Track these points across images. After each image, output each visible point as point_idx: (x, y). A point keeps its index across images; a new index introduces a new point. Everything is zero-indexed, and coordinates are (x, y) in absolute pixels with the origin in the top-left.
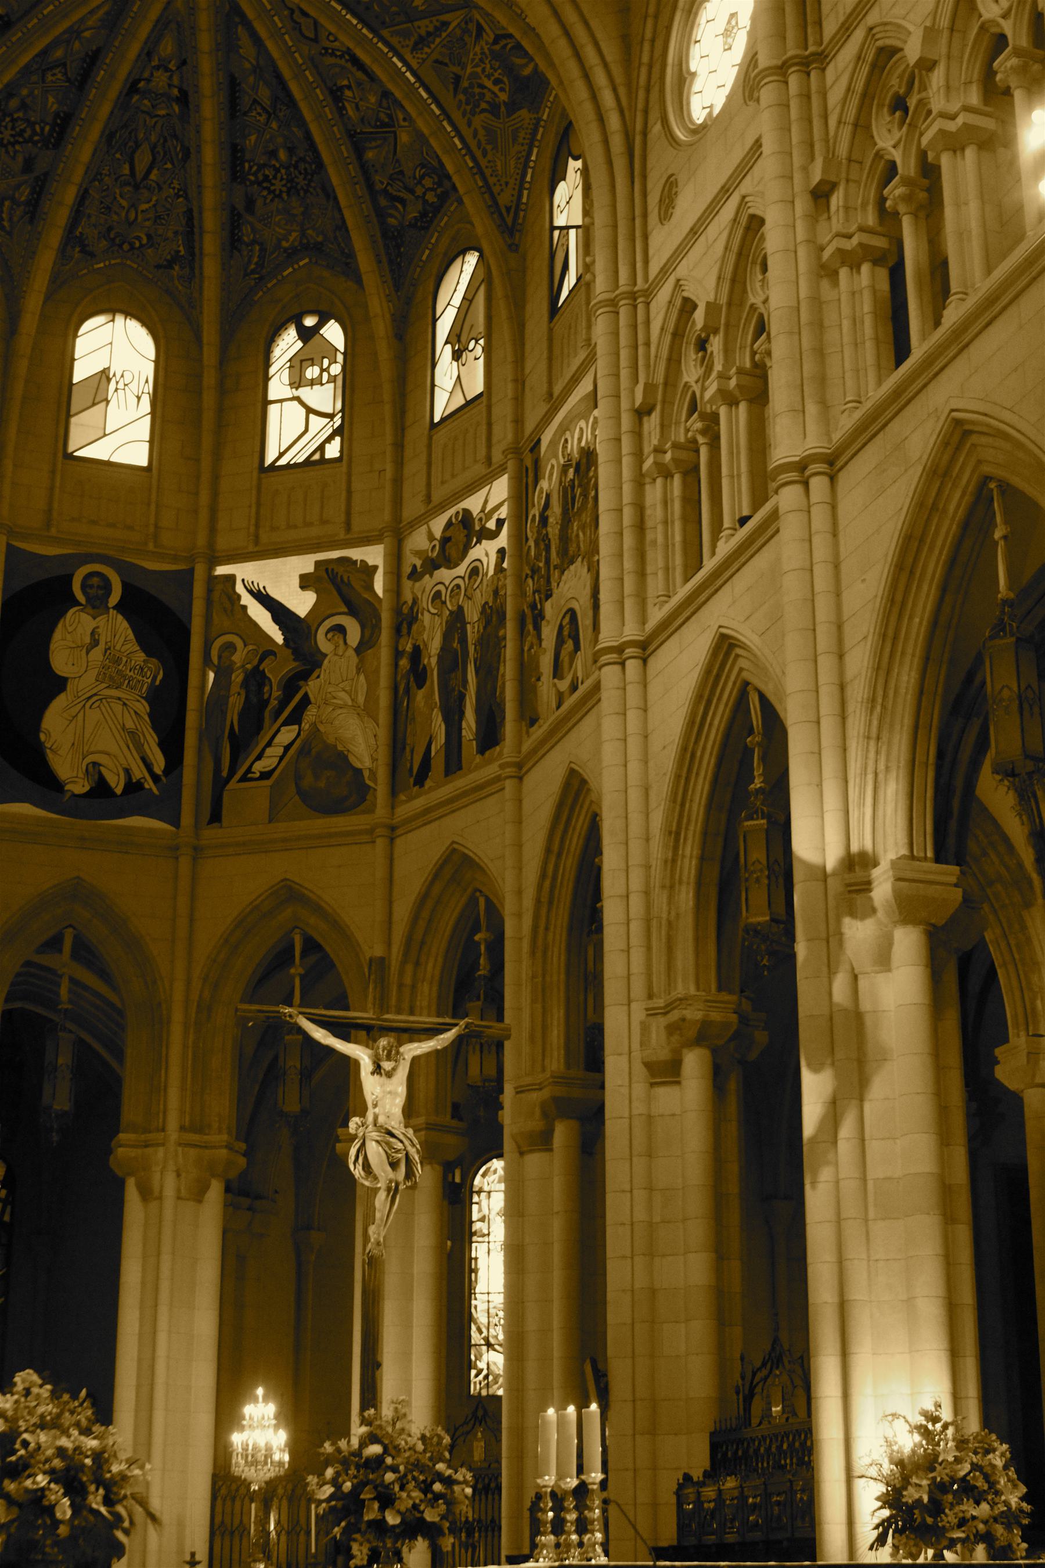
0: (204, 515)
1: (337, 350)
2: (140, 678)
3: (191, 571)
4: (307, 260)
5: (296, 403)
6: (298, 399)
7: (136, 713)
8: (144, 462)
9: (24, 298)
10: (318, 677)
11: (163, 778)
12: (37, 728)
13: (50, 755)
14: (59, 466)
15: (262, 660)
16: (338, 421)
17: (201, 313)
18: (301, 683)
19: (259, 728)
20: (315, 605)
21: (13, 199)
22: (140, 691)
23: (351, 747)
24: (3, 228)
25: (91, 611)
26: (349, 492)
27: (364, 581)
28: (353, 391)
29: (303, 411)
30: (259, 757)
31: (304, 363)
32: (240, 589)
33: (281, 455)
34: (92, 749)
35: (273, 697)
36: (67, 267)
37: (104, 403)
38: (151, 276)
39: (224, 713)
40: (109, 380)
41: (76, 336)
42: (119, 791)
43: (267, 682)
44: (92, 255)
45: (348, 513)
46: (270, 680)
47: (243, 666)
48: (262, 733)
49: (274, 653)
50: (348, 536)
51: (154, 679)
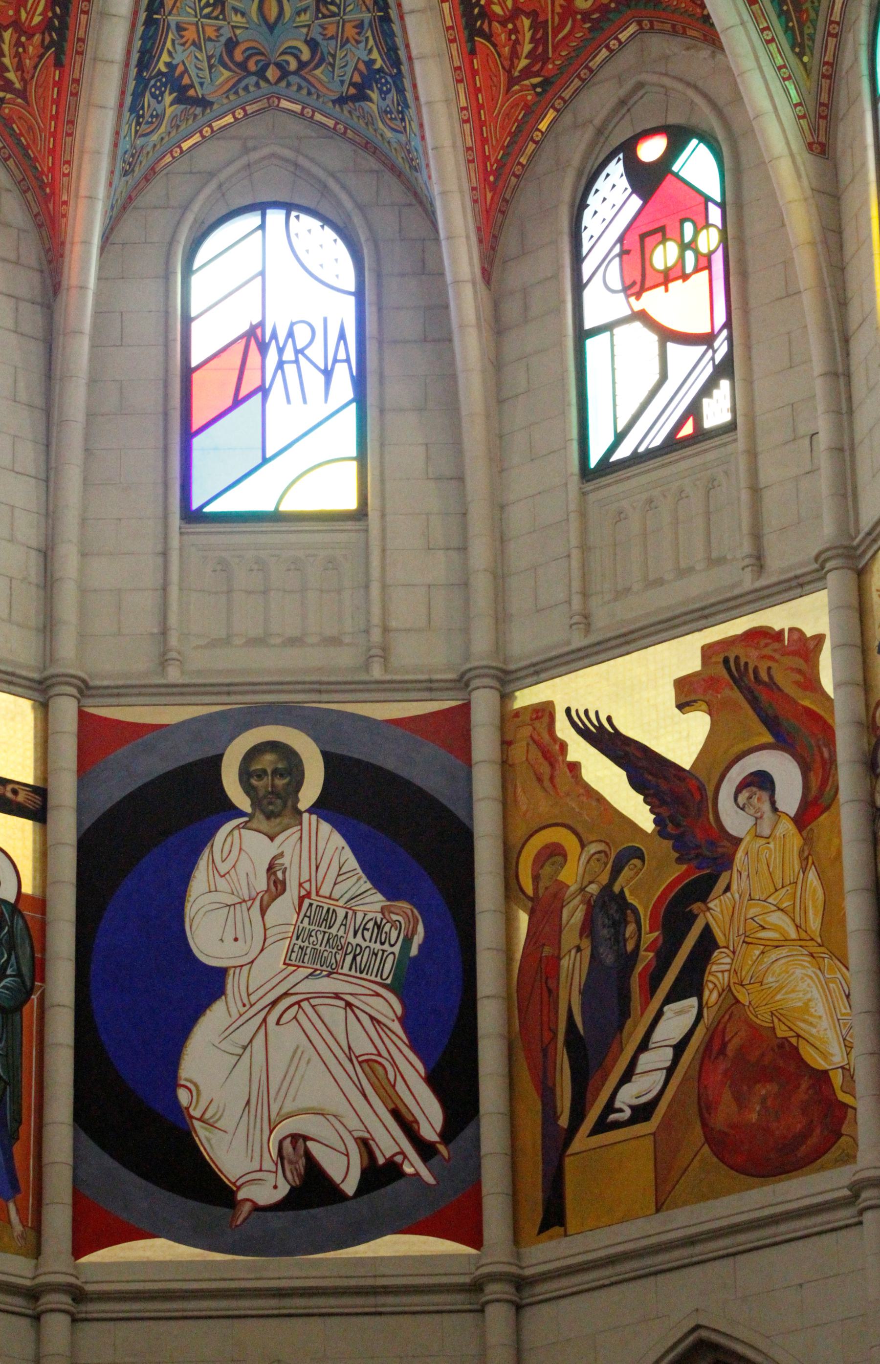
0: (482, 585)
1: (707, 199)
2: (378, 946)
3: (465, 709)
4: (632, 28)
5: (637, 325)
6: (642, 316)
7: (372, 1018)
8: (351, 504)
9: (64, 216)
10: (728, 889)
11: (441, 1148)
12: (172, 1081)
13: (201, 1133)
14: (175, 541)
15: (616, 872)
16: (721, 348)
17: (430, 177)
18: (696, 907)
19: (624, 1013)
20: (709, 737)
21: (16, 24)
22: (380, 971)
23: (802, 1027)
24: (8, 86)
25: (264, 825)
26: (756, 491)
27: (799, 671)
28: (744, 275)
29: (653, 339)
30: (627, 1076)
31: (649, 241)
32: (564, 730)
33: (620, 438)
34: (288, 1107)
35: (644, 945)
36: (155, 138)
37: (259, 395)
38: (331, 123)
39: (552, 993)
40: (263, 349)
41: (188, 271)
42: (350, 1187)
43: (630, 917)
44: (204, 103)
45: (757, 536)
46: (635, 911)
47: (582, 889)
48: (629, 1023)
49: (639, 854)
50: (758, 584)
51: (408, 941)
